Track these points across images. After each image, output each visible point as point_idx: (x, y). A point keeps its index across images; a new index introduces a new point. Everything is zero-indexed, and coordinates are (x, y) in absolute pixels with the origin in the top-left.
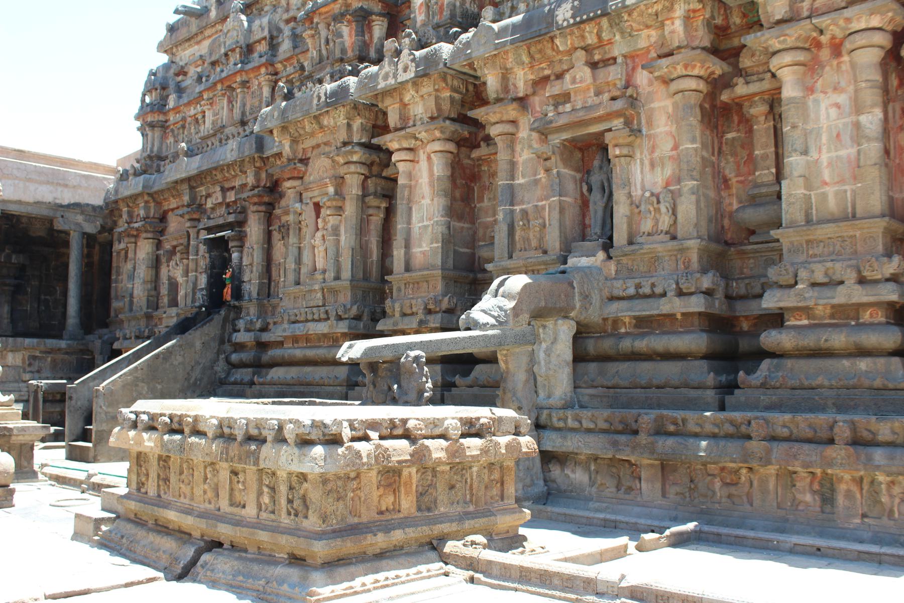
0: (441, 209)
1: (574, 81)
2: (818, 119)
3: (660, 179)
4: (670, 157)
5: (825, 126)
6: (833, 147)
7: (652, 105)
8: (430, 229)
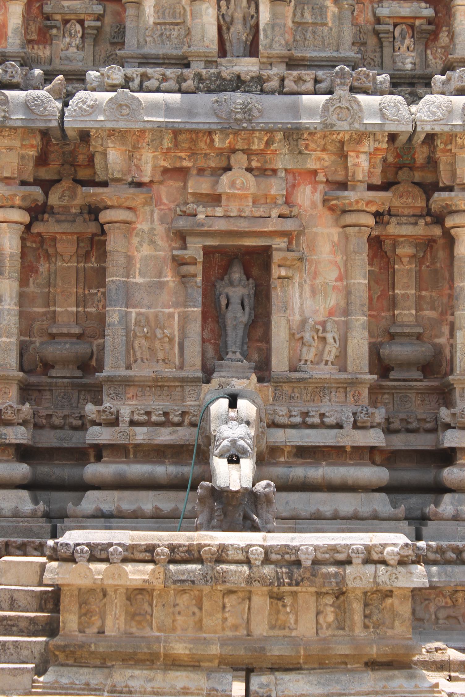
1: (233, 184)
3: (322, 308)
4: (334, 287)
7: (314, 229)
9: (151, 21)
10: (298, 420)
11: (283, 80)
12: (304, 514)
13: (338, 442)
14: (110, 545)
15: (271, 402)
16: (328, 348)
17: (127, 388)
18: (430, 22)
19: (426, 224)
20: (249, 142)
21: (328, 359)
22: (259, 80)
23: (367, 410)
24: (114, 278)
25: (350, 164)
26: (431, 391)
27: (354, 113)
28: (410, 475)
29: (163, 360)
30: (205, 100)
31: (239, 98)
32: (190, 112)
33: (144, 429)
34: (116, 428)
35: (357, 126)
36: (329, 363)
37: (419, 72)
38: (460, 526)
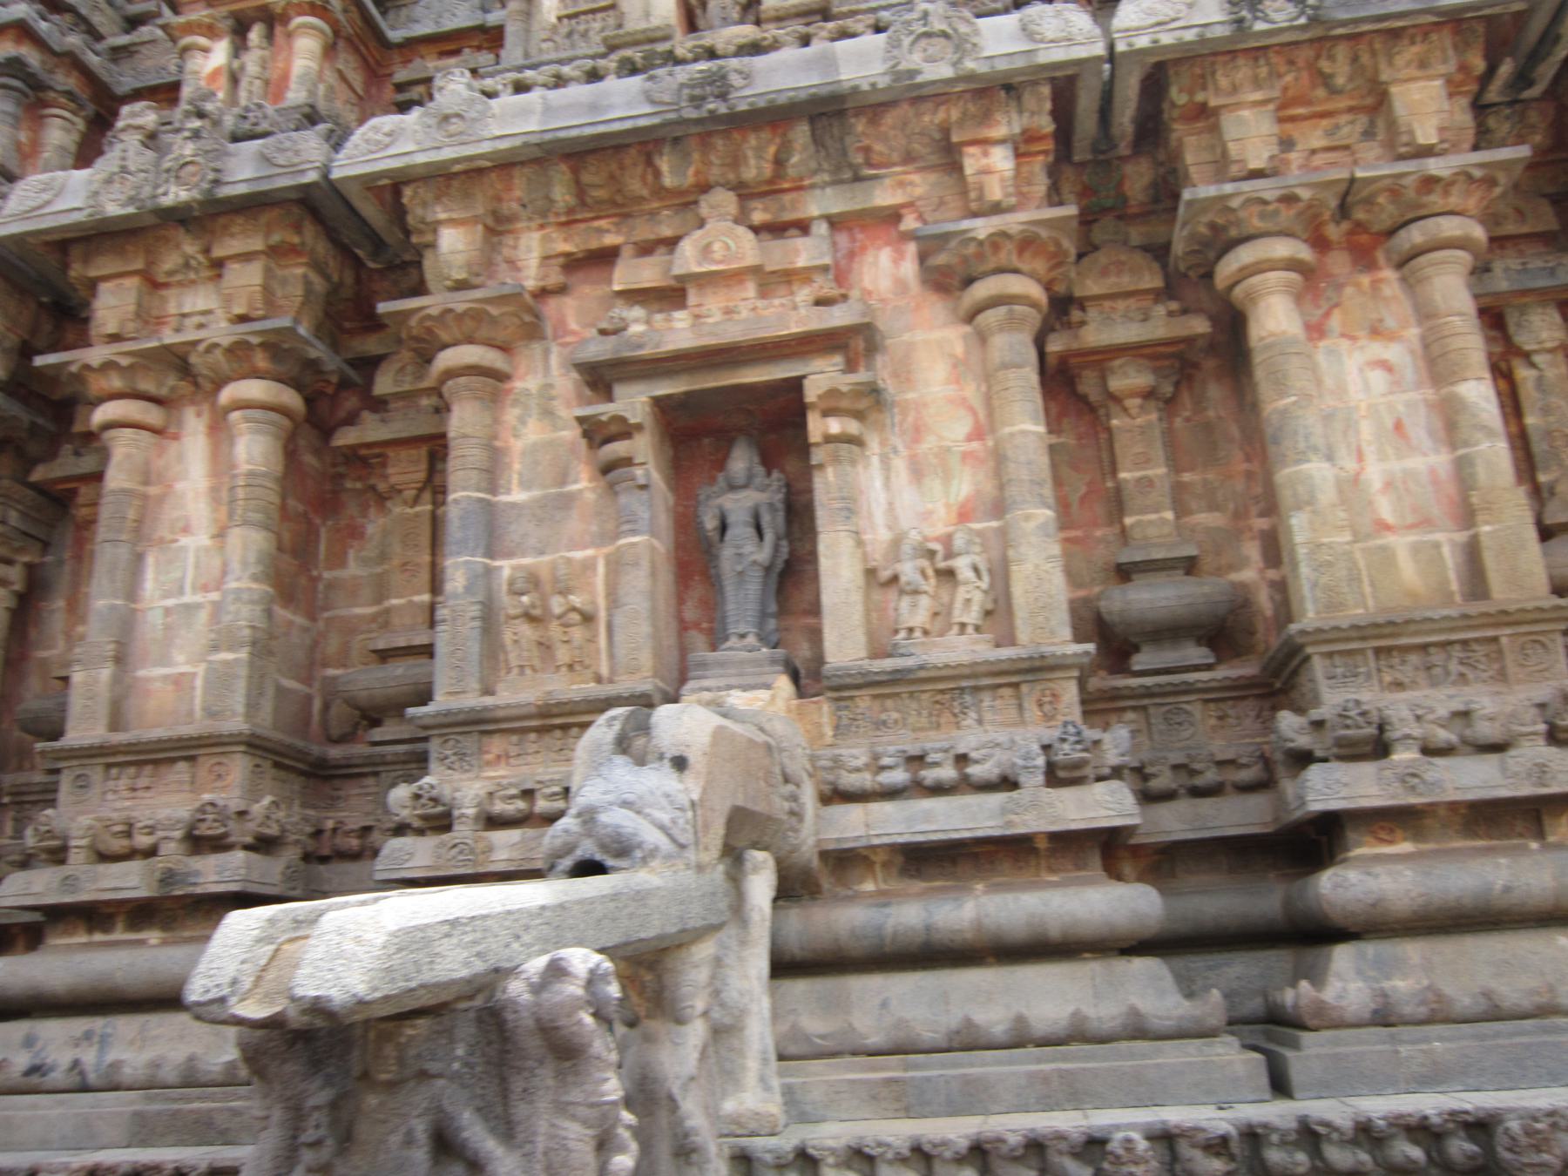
0: (252, 558)
2: (1341, 390)
4: (965, 456)
5: (1363, 405)
6: (1390, 451)
7: (906, 337)
8: (203, 616)
10: (899, 776)
12: (928, 1036)
13: (1009, 824)
15: (829, 739)
17: (485, 739)
19: (1171, 314)
21: (964, 620)
23: (1079, 733)
25: (968, 171)
26: (1238, 690)
28: (1221, 900)
29: (571, 667)
33: (514, 835)
34: (445, 837)
35: (970, 65)
36: (970, 629)
38: (1402, 1042)
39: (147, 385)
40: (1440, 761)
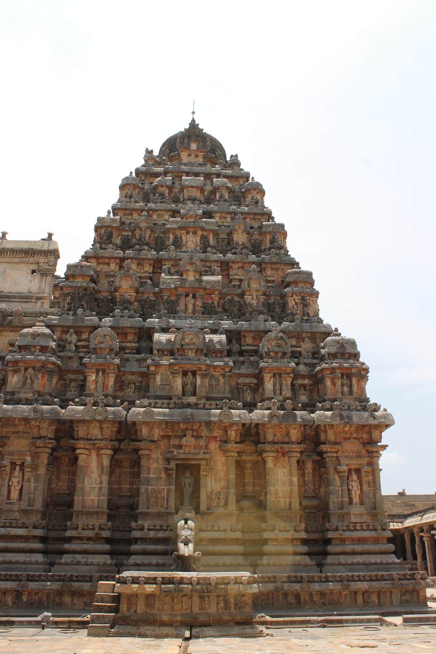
1: (187, 441)
8: (97, 489)
9: (159, 384)
11: (205, 404)
14: (140, 577)
16: (221, 502)
18: (256, 384)
20: (193, 426)
22: (196, 404)
24: (143, 475)
27: (230, 416)
30: (178, 411)
31: (189, 411)
32: (172, 415)
33: (153, 532)
35: (231, 421)
37: (252, 402)
39: (87, 447)
40: (281, 532)
